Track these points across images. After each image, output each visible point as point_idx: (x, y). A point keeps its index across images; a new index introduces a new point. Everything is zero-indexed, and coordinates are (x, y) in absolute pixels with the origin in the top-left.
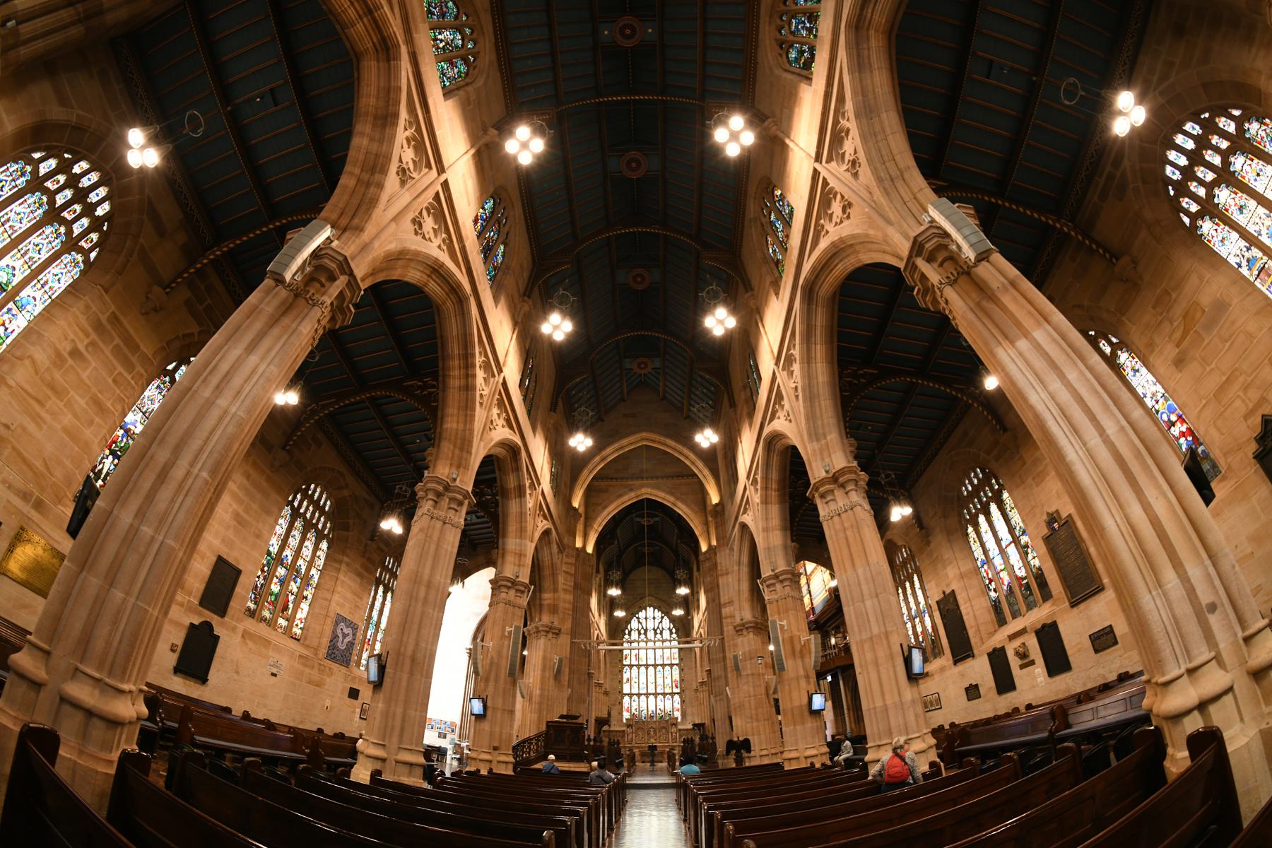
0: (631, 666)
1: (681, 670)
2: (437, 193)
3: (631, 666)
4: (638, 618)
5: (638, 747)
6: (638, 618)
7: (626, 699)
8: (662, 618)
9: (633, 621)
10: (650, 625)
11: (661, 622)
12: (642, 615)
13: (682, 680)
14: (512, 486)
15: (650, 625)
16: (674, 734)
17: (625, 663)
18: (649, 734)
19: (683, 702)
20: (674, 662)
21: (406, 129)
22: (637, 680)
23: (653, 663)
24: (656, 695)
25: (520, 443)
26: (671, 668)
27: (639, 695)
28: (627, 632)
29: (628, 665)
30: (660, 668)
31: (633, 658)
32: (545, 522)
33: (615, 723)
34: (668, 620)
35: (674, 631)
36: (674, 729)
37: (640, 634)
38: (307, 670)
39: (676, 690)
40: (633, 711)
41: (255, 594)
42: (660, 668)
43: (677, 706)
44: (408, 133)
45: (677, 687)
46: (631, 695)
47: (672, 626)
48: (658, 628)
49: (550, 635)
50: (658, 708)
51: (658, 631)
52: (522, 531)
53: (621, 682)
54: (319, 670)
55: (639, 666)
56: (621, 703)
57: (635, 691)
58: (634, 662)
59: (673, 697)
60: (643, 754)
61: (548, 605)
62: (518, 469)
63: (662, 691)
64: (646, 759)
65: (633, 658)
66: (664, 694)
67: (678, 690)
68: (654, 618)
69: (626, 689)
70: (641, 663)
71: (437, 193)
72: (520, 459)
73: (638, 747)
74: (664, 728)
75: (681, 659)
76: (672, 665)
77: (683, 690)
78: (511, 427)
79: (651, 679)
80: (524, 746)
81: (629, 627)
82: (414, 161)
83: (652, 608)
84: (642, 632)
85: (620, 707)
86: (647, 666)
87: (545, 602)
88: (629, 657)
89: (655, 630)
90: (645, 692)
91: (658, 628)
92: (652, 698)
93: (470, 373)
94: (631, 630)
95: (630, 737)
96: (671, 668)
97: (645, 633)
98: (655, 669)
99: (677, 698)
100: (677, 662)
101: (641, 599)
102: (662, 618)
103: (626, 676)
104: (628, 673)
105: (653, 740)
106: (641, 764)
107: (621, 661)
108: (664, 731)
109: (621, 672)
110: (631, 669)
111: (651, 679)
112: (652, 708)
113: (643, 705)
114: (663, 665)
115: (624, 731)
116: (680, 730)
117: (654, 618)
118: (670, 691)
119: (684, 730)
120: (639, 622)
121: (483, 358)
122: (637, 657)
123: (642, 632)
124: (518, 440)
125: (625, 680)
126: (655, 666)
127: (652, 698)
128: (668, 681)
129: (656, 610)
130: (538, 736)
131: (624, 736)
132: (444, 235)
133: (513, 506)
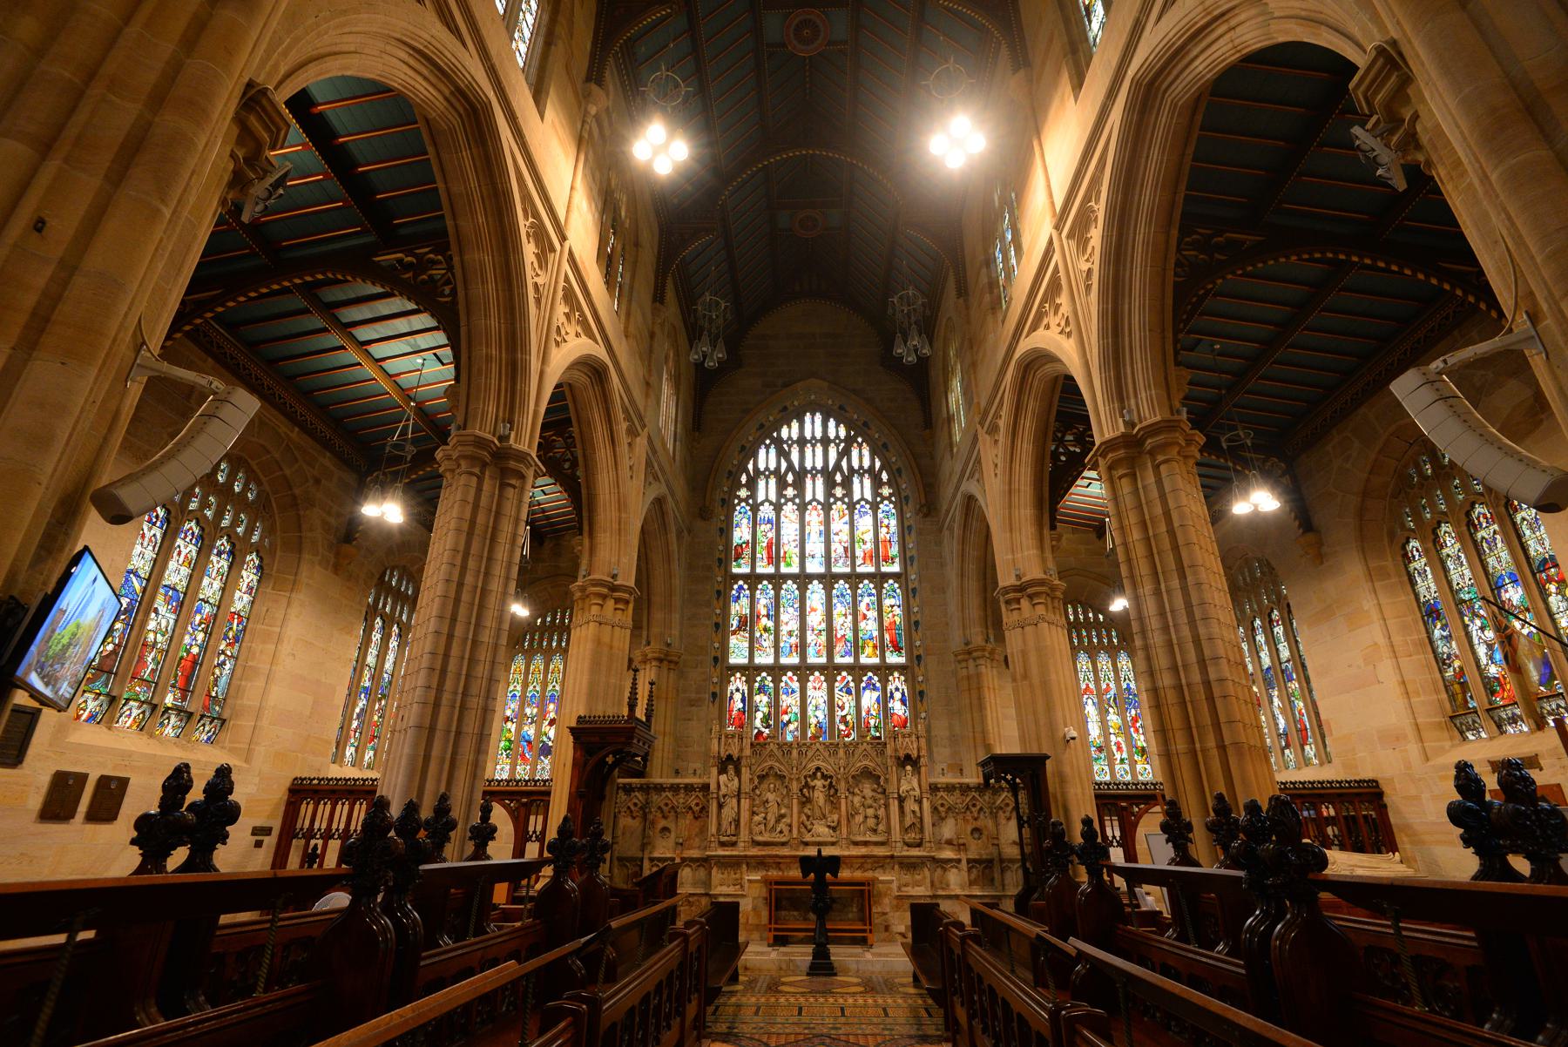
1: (909, 594)
3: (753, 579)
4: (778, 443)
5: (760, 863)
6: (778, 443)
7: (737, 683)
8: (849, 441)
9: (762, 452)
10: (814, 458)
11: (845, 453)
12: (790, 431)
13: (912, 624)
15: (814, 458)
16: (911, 806)
17: (735, 570)
18: (806, 801)
19: (916, 697)
20: (885, 569)
22: (770, 624)
23: (822, 570)
24: (830, 671)
26: (879, 588)
27: (777, 670)
28: (744, 479)
29: (744, 577)
30: (841, 585)
31: (761, 553)
32: (584, 339)
33: (698, 765)
34: (866, 452)
35: (885, 476)
36: (909, 783)
37: (781, 484)
39: (893, 658)
42: (841, 585)
43: (897, 708)
45: (897, 649)
46: (750, 671)
47: (878, 464)
48: (838, 467)
50: (840, 713)
51: (838, 478)
53: (721, 628)
55: (777, 580)
56: (719, 698)
57: (765, 658)
58: (764, 568)
59: (884, 682)
60: (780, 899)
63: (849, 660)
64: (794, 920)
65: (761, 553)
66: (857, 670)
67: (902, 660)
68: (825, 441)
69: (738, 651)
70: (784, 569)
73: (760, 863)
74: (867, 774)
75: (905, 560)
76: (879, 578)
77: (916, 659)
78: (591, 336)
79: (816, 619)
81: (750, 467)
83: (818, 418)
84: (790, 478)
85: (714, 710)
86: (803, 579)
88: (747, 552)
89: (828, 475)
90: (794, 660)
92: (816, 680)
95: (728, 812)
96: (879, 588)
97: (799, 484)
98: (828, 589)
99: (897, 683)
100: (896, 568)
101: (786, 385)
102: (849, 441)
103: (740, 608)
104: (745, 601)
105: (821, 830)
106: (774, 955)
107: (724, 562)
108: (867, 788)
109: (723, 597)
110: (753, 589)
111: (816, 619)
112: (817, 715)
113: (790, 701)
114: (854, 579)
115: (706, 787)
116: (934, 788)
117: (825, 441)
118: (876, 660)
119: (950, 788)
120: (783, 454)
122: (775, 556)
123: (790, 478)
124: (600, 352)
125: (735, 623)
126: (828, 579)
127: (816, 684)
128: (870, 627)
129: (832, 423)
131: (704, 809)
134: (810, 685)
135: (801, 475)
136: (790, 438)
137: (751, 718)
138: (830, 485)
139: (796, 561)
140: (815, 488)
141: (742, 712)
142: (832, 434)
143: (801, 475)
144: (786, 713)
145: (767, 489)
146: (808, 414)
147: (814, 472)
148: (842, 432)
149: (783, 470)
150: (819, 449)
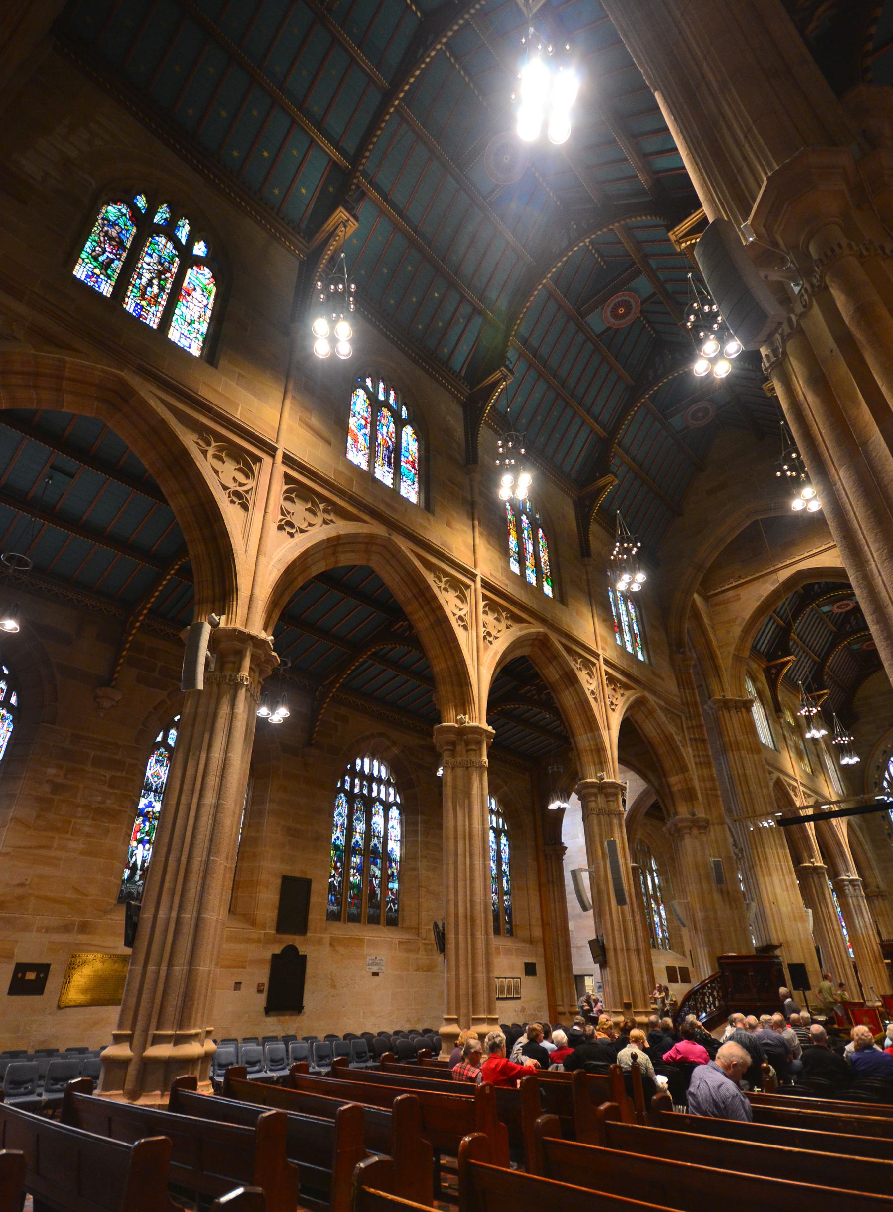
2: (286, 476)
14: (557, 677)
21: (205, 453)
25: (541, 629)
38: (413, 956)
41: (335, 895)
44: (211, 451)
49: (695, 831)
52: (591, 724)
54: (426, 951)
61: (679, 790)
62: (555, 657)
71: (286, 476)
72: (552, 645)
80: (695, 1000)
82: (239, 470)
87: (675, 789)
93: (434, 606)
121: (444, 579)
130: (712, 979)
132: (322, 506)
133: (567, 699)
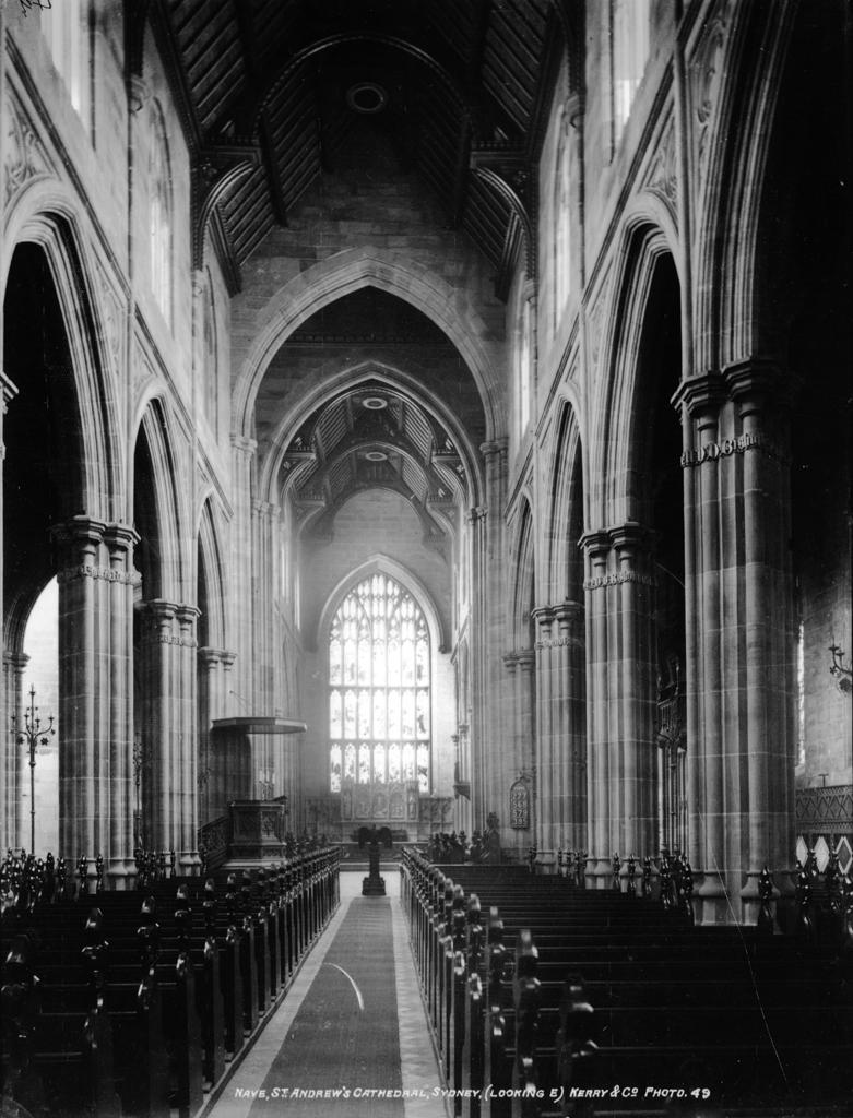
0: (343, 689)
4: (357, 597)
37: (359, 627)
40: (347, 772)
46: (343, 743)
48: (393, 616)
51: (393, 623)
57: (350, 735)
69: (335, 732)
70: (361, 683)
83: (382, 579)
84: (364, 622)
91: (393, 616)
94: (344, 619)
123: (364, 622)
129: (390, 584)
134: (375, 751)
135: (371, 620)
136: (363, 594)
137: (343, 769)
138: (389, 627)
139: (368, 675)
140: (379, 629)
141: (338, 766)
142: (390, 592)
143: (371, 620)
144: (362, 765)
145: (349, 630)
146: (375, 580)
147: (380, 618)
148: (397, 592)
149: (359, 617)
150: (382, 603)
